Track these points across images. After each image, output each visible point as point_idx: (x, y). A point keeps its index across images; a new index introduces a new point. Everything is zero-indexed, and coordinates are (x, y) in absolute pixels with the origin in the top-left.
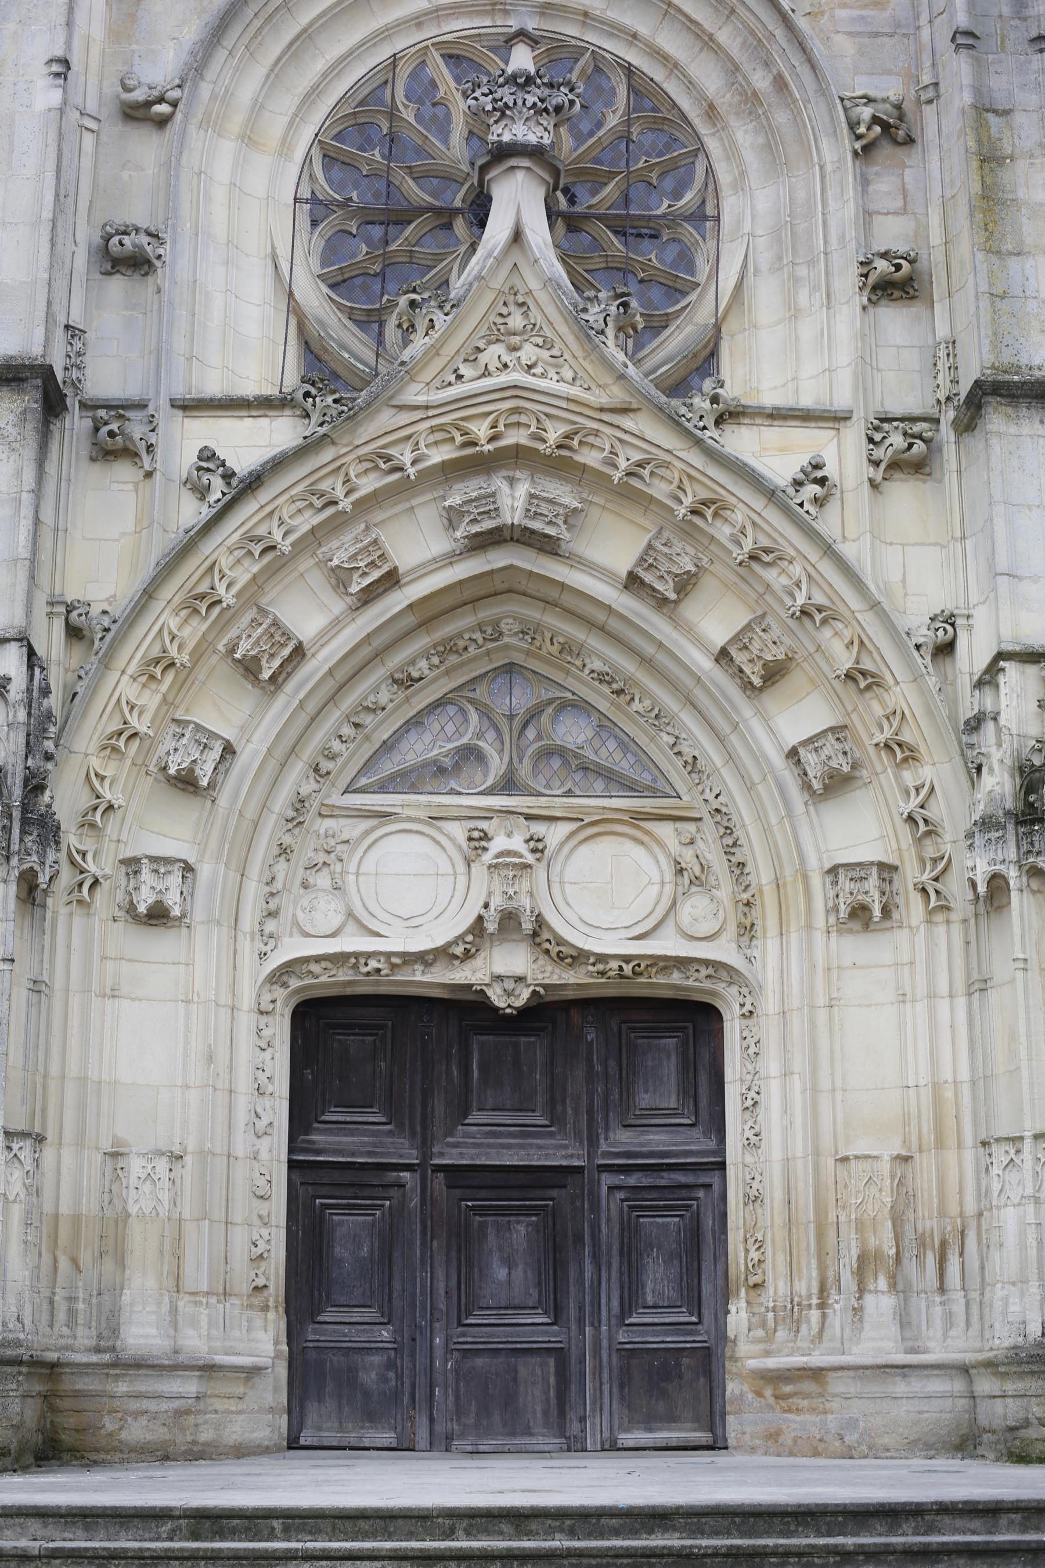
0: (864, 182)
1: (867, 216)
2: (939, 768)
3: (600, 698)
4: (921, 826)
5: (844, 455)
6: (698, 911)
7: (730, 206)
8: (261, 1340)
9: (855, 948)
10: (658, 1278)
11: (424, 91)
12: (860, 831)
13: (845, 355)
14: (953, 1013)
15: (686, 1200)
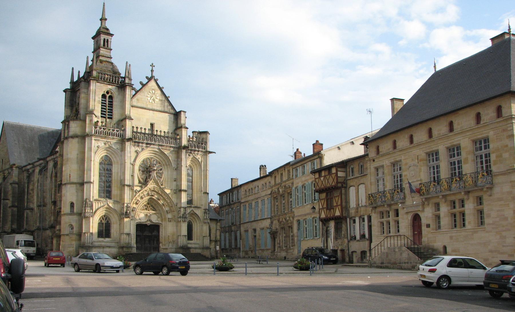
8: (135, 246)
9: (169, 223)
10: (155, 242)
12: (169, 216)
14: (175, 227)
15: (157, 237)
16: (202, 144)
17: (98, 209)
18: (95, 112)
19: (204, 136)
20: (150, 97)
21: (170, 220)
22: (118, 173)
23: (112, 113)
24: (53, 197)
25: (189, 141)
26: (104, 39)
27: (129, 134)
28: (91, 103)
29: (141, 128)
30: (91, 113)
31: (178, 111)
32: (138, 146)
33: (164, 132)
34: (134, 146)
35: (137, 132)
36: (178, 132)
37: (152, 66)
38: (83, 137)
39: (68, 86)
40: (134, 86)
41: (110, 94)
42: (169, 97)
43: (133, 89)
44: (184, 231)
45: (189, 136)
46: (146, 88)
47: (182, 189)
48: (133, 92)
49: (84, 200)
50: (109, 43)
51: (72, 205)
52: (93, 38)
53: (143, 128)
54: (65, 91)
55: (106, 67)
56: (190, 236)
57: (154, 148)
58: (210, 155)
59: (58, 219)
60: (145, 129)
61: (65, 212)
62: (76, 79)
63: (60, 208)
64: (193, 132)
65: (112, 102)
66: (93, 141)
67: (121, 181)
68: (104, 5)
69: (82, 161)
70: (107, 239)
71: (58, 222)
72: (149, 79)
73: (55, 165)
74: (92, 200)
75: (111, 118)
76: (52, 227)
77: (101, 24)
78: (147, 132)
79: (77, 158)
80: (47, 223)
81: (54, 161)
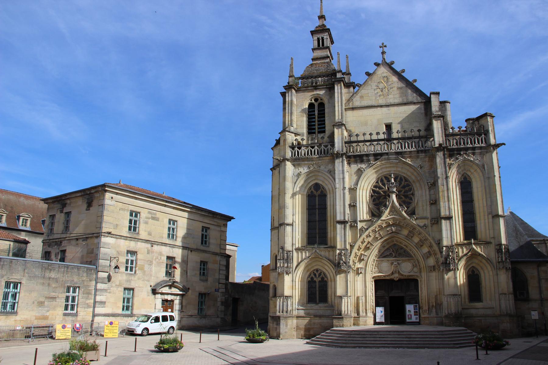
0: (430, 191)
1: (430, 195)
2: (439, 255)
3: (405, 247)
4: (437, 261)
6: (415, 269)
7: (416, 193)
12: (431, 261)
13: (428, 211)
16: (480, 135)
32: (362, 161)
41: (319, 101)
46: (375, 78)
47: (443, 214)
53: (368, 133)
55: (316, 70)
57: (388, 159)
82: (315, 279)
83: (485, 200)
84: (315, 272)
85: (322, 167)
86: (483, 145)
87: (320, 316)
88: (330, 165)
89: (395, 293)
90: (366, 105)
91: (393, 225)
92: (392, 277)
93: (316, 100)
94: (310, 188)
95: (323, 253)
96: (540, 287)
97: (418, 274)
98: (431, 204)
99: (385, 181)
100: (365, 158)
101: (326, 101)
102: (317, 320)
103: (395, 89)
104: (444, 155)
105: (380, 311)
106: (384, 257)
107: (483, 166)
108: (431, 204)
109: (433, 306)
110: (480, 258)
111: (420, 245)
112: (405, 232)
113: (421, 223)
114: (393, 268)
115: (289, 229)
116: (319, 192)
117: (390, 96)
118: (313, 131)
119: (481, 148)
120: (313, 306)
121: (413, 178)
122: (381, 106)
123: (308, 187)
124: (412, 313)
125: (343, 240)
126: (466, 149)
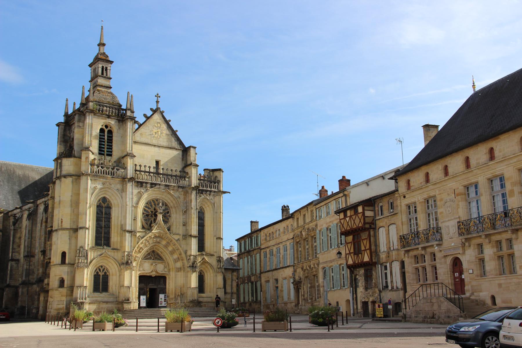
2: (185, 261)
3: (160, 253)
4: (183, 265)
5: (181, 237)
6: (166, 270)
7: (172, 215)
11: (151, 203)
12: (179, 265)
16: (215, 183)
17: (94, 259)
18: (91, 149)
19: (216, 174)
20: (155, 131)
21: (179, 270)
22: (118, 217)
23: (112, 149)
24: (43, 246)
25: (200, 180)
26: (103, 67)
27: (130, 173)
28: (87, 139)
29: (145, 166)
30: (87, 149)
31: (187, 146)
32: (142, 186)
33: (172, 170)
34: (137, 186)
35: (140, 171)
36: (187, 170)
37: (157, 96)
38: (78, 176)
39: (62, 120)
40: (136, 119)
41: (109, 128)
42: (177, 131)
43: (136, 122)
44: (194, 282)
45: (200, 174)
46: (151, 121)
48: (136, 126)
49: (78, 248)
50: (108, 71)
51: (64, 254)
52: (90, 66)
53: (148, 166)
54: (58, 125)
56: (201, 288)
58: (224, 195)
59: (47, 272)
60: (149, 167)
61: (55, 263)
62: (70, 111)
63: (50, 259)
64: (204, 170)
65: (112, 137)
66: (89, 181)
67: (122, 226)
68: (102, 29)
69: (76, 203)
70: (104, 294)
71: (46, 275)
72: (154, 111)
73: (46, 209)
74: (86, 248)
75: (111, 155)
76: (40, 281)
77: (99, 50)
78: (152, 170)
79: (71, 200)
80: (35, 276)
81: (45, 204)
82: (100, 273)
83: (212, 226)
84: (100, 268)
85: (113, 186)
86: (216, 190)
87: (107, 302)
88: (118, 185)
89: (152, 286)
90: (144, 142)
91: (159, 237)
92: (151, 274)
93: (106, 127)
94: (99, 201)
95: (109, 253)
96: (232, 285)
97: (167, 273)
98: (184, 225)
99: (153, 203)
100: (144, 184)
101: (115, 130)
102: (104, 306)
103: (164, 135)
104: (196, 193)
105: (143, 298)
106: (146, 259)
107: (214, 204)
108: (184, 225)
109: (178, 295)
110: (207, 264)
111: (172, 253)
112: (164, 243)
113: (176, 237)
114: (152, 267)
115: (87, 231)
116: (106, 204)
117: (161, 139)
118: (103, 153)
119: (215, 192)
120: (97, 294)
121: (172, 204)
122: (155, 146)
123: (98, 199)
124: (163, 300)
125: (130, 245)
126: (207, 191)
